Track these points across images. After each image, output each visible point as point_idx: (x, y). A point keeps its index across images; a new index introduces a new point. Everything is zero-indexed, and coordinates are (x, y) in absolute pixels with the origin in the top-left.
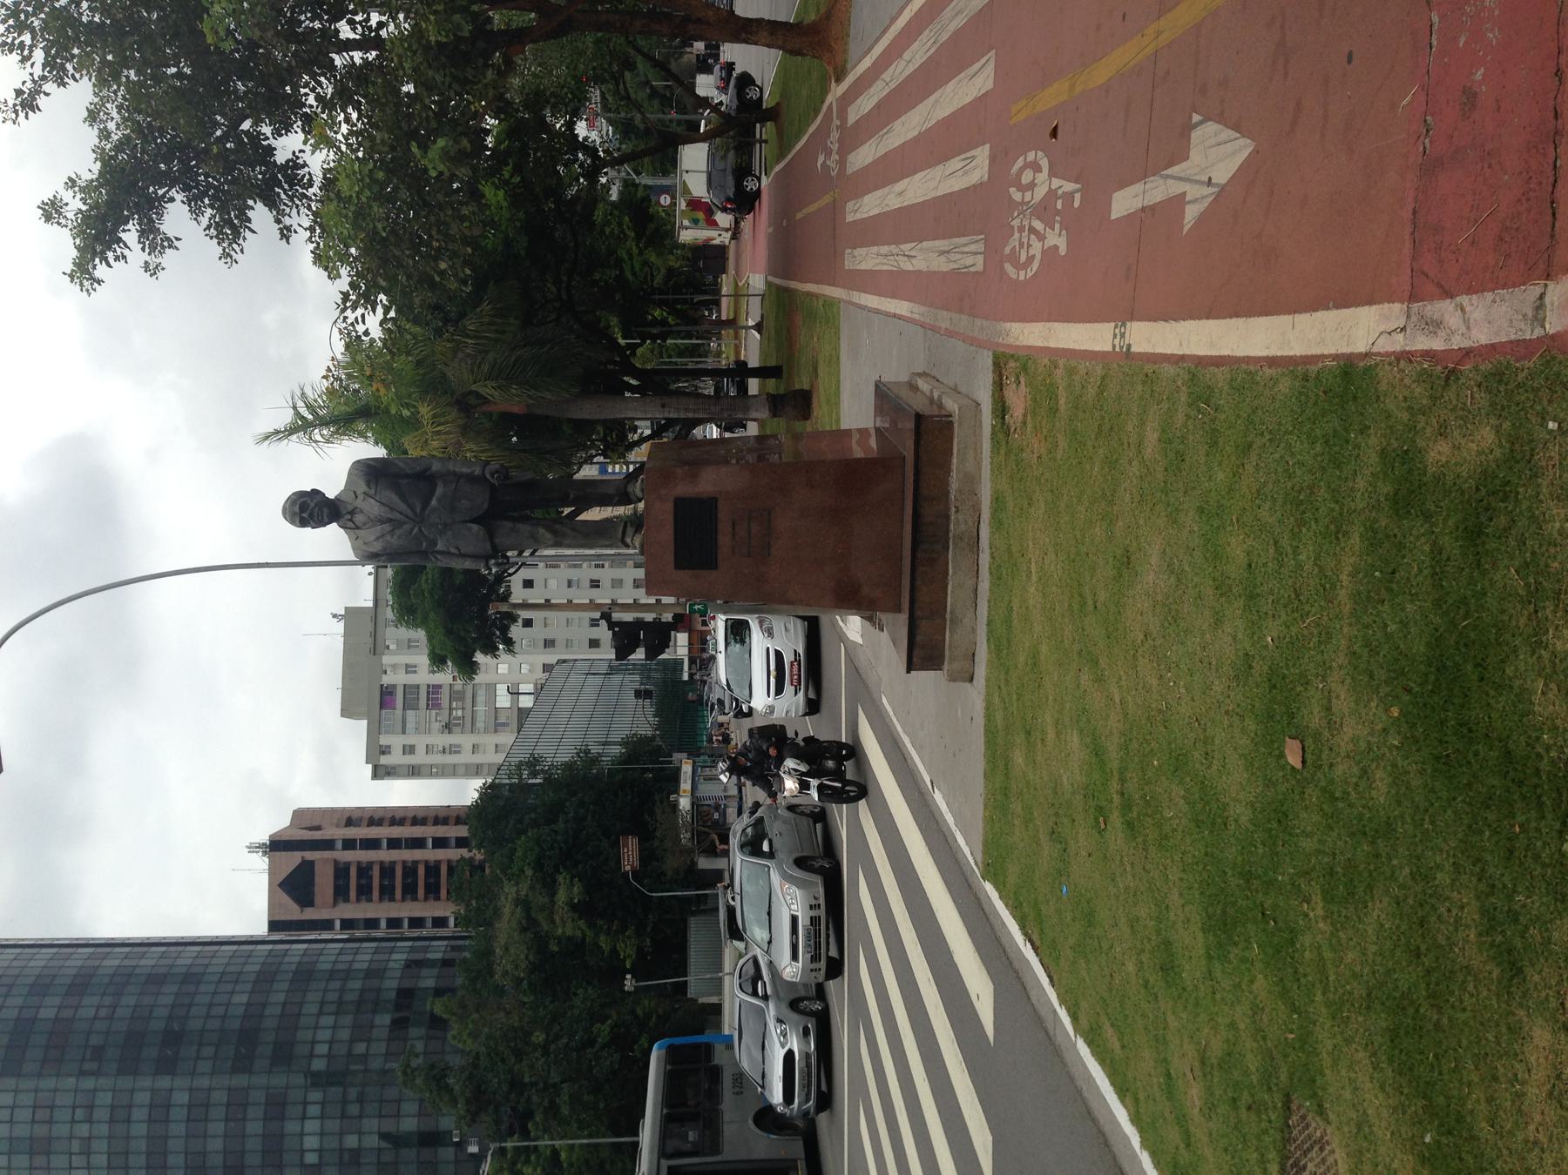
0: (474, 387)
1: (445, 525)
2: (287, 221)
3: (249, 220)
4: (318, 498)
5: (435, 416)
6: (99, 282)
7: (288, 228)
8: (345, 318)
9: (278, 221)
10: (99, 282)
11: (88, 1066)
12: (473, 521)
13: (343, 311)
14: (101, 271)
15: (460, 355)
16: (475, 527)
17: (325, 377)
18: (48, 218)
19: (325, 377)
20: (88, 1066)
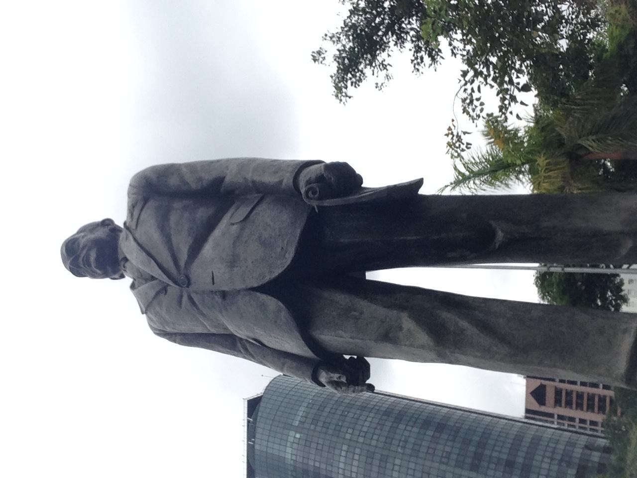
0: (579, 142)
1: (224, 295)
2: (456, 43)
3: (440, 51)
4: (101, 233)
5: (549, 164)
6: (350, 97)
7: (454, 48)
8: (465, 90)
9: (450, 44)
10: (350, 97)
11: (444, 460)
12: (264, 289)
13: (465, 84)
14: (351, 90)
15: (571, 119)
16: (272, 303)
17: (447, 135)
18: (315, 60)
19: (447, 135)
20: (444, 460)
